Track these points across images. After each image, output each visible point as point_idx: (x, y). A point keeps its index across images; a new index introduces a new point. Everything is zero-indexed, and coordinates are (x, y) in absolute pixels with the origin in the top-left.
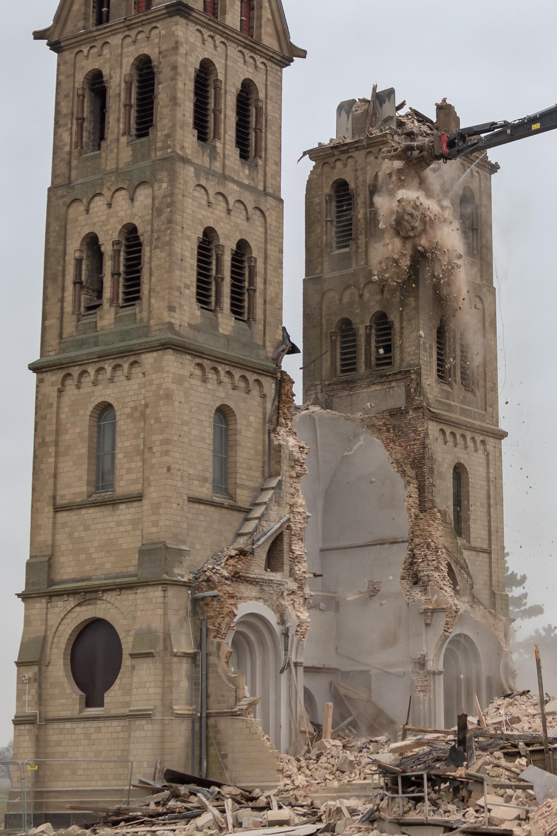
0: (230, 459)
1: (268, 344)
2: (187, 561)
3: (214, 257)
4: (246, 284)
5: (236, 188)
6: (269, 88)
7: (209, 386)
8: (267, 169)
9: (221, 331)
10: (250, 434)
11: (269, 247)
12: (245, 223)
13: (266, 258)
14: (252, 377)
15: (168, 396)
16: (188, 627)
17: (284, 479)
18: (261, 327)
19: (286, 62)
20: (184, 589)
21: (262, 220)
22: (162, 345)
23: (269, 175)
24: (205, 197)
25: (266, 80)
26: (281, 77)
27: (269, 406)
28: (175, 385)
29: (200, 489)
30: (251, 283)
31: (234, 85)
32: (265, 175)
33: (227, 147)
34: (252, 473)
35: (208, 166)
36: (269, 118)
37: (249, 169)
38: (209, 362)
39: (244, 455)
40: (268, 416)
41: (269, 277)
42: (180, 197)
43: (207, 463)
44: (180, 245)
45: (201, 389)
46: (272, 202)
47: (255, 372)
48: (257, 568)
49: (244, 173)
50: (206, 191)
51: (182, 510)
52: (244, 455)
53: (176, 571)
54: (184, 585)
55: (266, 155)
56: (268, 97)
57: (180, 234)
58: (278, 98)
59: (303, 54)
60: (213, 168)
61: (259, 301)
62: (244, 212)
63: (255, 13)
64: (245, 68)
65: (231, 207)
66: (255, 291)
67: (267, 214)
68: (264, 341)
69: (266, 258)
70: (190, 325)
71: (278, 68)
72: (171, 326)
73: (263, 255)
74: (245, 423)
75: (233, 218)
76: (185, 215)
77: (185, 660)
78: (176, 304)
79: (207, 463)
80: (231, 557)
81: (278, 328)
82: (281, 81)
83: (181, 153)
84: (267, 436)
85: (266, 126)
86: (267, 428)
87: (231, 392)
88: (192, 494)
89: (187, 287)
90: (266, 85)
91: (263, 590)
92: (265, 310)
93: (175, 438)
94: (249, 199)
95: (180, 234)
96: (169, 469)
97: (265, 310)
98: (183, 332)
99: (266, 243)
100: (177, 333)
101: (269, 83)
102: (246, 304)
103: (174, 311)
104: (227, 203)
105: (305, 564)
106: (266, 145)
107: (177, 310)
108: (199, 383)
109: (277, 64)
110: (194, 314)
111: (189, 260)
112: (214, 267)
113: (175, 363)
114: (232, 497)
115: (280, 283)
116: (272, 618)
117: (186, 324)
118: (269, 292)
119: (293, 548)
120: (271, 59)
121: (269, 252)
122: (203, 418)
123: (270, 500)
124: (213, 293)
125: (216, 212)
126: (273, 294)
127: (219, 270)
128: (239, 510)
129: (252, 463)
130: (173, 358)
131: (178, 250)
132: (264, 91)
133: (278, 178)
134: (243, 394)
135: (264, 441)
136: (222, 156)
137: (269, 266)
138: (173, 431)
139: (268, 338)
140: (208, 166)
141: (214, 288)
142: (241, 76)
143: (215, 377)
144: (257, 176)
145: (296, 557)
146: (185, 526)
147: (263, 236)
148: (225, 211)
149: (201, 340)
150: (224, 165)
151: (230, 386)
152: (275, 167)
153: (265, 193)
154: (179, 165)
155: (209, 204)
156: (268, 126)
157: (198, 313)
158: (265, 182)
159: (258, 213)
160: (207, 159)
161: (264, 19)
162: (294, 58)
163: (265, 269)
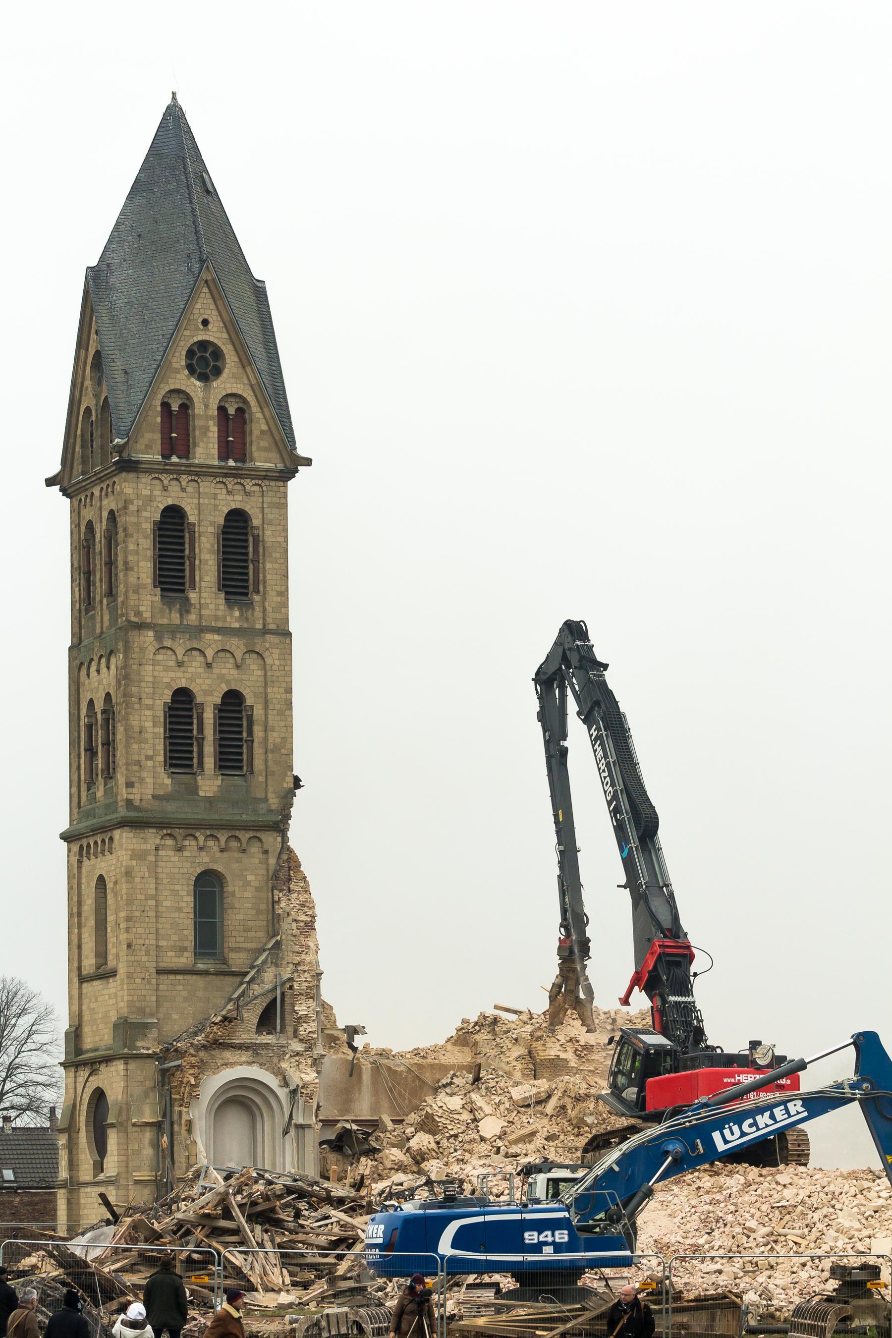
0: (225, 923)
1: (270, 795)
2: (153, 1034)
3: (195, 716)
4: (245, 735)
5: (216, 637)
6: (266, 510)
7: (186, 854)
9: (201, 794)
11: (269, 690)
12: (234, 672)
14: (244, 836)
15: (128, 874)
16: (154, 1097)
17: (284, 937)
18: (261, 779)
19: (289, 473)
20: (149, 1061)
21: (260, 661)
22: (119, 823)
23: (269, 609)
24: (174, 657)
25: (263, 502)
26: (286, 494)
27: (272, 861)
28: (134, 863)
29: (176, 960)
30: (250, 733)
31: (212, 523)
32: (264, 610)
33: (204, 595)
35: (178, 622)
36: (268, 544)
37: (240, 610)
38: (181, 831)
39: (238, 917)
40: (271, 873)
41: (270, 723)
42: (135, 667)
43: (185, 932)
44: (137, 717)
45: (176, 859)
46: (275, 639)
47: (250, 830)
48: (247, 1033)
49: (232, 616)
50: (173, 651)
51: (149, 983)
52: (238, 917)
53: (139, 1044)
54: (149, 1056)
55: (265, 587)
56: (266, 522)
57: (137, 706)
58: (282, 518)
59: (308, 462)
60: (185, 622)
61: (258, 751)
62: (232, 660)
63: (247, 427)
64: (230, 498)
65: (210, 660)
66: (252, 741)
67: (266, 655)
68: (266, 793)
70: (154, 797)
71: (281, 484)
72: (129, 803)
73: (262, 700)
74: (241, 883)
75: (215, 671)
76: (143, 684)
77: (148, 1129)
78: (133, 779)
79: (185, 932)
80: (216, 1024)
81: (286, 776)
82: (286, 497)
83: (136, 620)
84: (270, 894)
85: (264, 556)
86: (270, 885)
87: (218, 854)
88: (163, 965)
89: (149, 758)
90: (263, 508)
91: (257, 1053)
92: (266, 761)
93: (137, 914)
94: (237, 645)
95: (137, 706)
96: (129, 946)
97: (266, 761)
99: (266, 686)
100: (138, 809)
101: (265, 506)
102: (245, 757)
103: (133, 787)
104: (205, 656)
105: (312, 1024)
106: (264, 577)
107: (136, 785)
108: (171, 853)
109: (276, 480)
110: (163, 784)
111: (150, 730)
112: (195, 727)
113: (134, 840)
114: (225, 962)
115: (289, 727)
116: (272, 1081)
117: (150, 797)
118: (270, 740)
119: (296, 1008)
120: (265, 478)
121: (269, 696)
122: (178, 887)
123: (264, 962)
124: (195, 755)
125: (190, 670)
126: (278, 740)
127: (201, 730)
128: (234, 974)
129: (251, 923)
130: (131, 835)
131: (135, 723)
132: (260, 516)
133: (283, 610)
134: (236, 855)
135: (268, 898)
136: (198, 606)
137: (270, 712)
138: (134, 907)
139: (270, 789)
140: (178, 622)
141: (195, 749)
142: (224, 508)
143: (194, 843)
144: (253, 615)
145: (300, 1018)
146: (154, 998)
147: (262, 679)
148: (204, 665)
149: (171, 809)
150: (200, 616)
151: (216, 849)
152: (279, 599)
153: (265, 631)
154: (133, 635)
155: (180, 664)
156: (267, 555)
157: (168, 781)
158: (264, 619)
159: (254, 656)
161: (256, 433)
162: (299, 468)
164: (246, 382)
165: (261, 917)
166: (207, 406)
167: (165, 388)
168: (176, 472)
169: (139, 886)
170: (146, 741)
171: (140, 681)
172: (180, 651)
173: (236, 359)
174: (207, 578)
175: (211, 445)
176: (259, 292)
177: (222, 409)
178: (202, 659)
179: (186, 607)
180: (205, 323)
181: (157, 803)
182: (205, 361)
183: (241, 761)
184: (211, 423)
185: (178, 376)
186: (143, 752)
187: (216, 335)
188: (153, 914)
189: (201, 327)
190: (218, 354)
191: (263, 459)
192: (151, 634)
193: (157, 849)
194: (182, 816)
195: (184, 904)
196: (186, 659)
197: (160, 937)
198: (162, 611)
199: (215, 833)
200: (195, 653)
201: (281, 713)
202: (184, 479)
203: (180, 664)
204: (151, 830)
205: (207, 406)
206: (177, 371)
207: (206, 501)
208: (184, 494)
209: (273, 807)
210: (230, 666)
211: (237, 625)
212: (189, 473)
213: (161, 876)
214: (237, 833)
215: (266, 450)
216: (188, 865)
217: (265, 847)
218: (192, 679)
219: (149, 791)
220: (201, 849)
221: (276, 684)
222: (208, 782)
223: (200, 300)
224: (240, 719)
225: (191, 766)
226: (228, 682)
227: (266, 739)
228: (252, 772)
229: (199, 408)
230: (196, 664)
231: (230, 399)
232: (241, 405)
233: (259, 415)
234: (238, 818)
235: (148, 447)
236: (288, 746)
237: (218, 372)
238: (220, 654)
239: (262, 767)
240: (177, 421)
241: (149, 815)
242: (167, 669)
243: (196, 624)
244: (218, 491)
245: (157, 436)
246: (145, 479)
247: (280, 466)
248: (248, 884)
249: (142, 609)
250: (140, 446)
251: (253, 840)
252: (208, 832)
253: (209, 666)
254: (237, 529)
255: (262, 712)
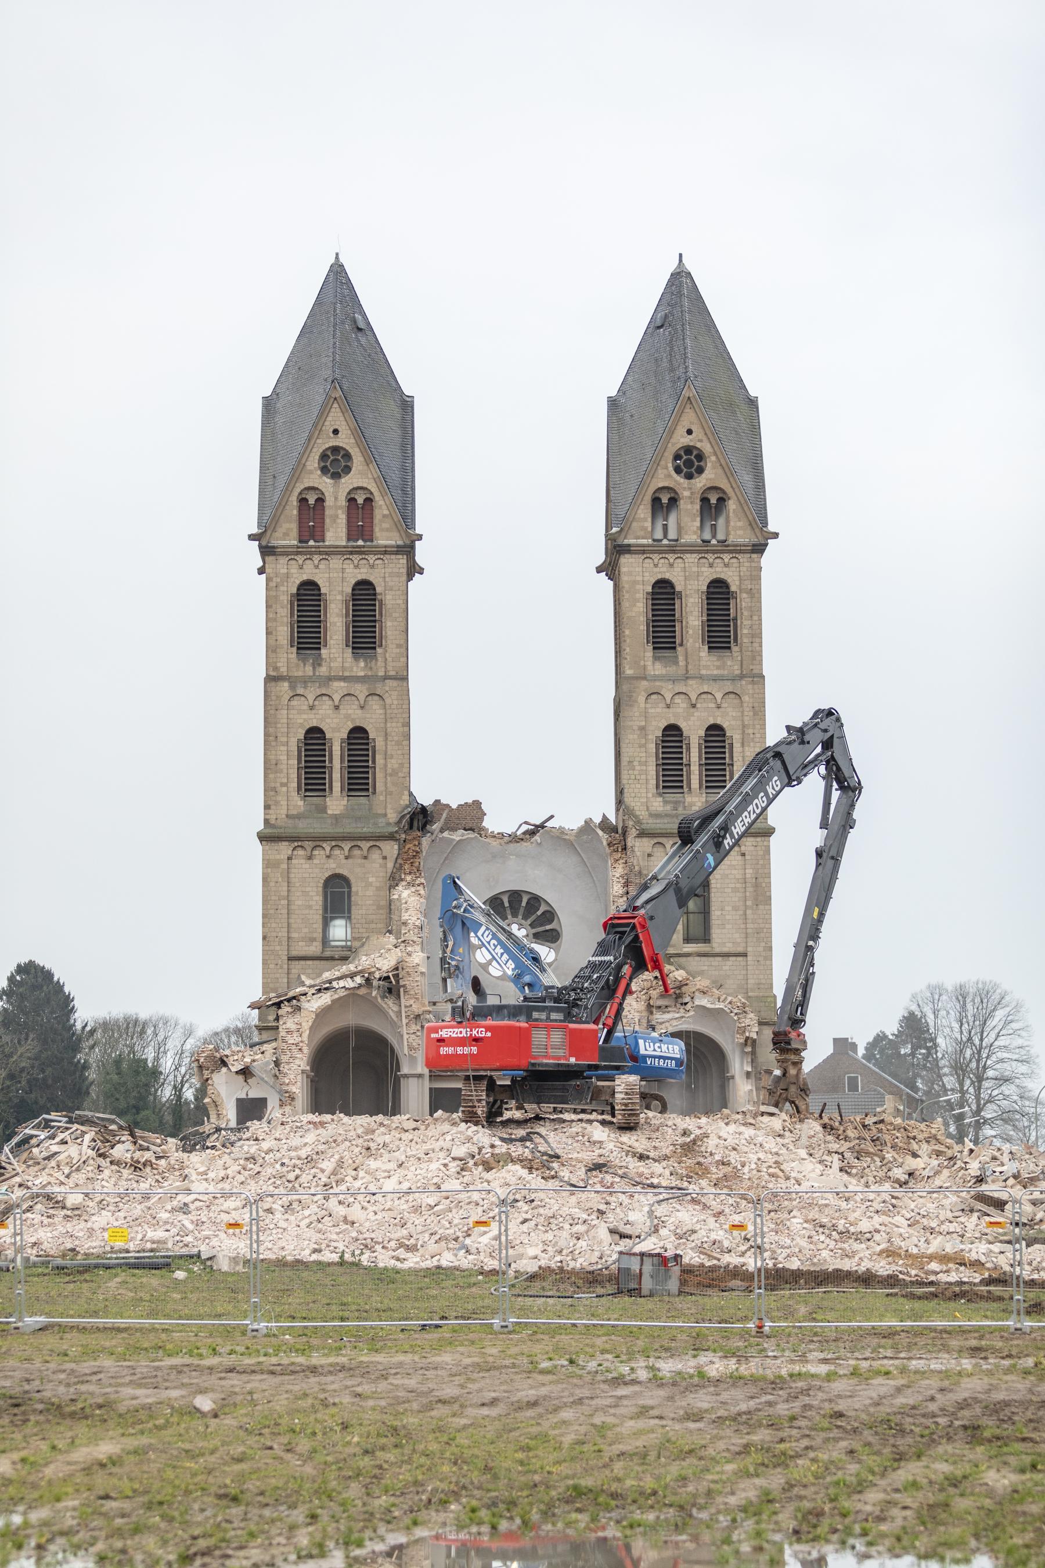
1: (389, 811)
5: (342, 684)
7: (315, 861)
8: (387, 655)
9: (329, 812)
10: (368, 893)
11: (389, 725)
12: (359, 712)
13: (386, 734)
14: (365, 845)
18: (382, 798)
21: (381, 702)
23: (389, 659)
27: (390, 865)
28: (269, 870)
29: (307, 948)
30: (374, 762)
34: (373, 926)
35: (311, 674)
37: (365, 661)
39: (360, 912)
40: (389, 875)
43: (315, 926)
45: (307, 866)
46: (394, 683)
51: (281, 968)
52: (360, 912)
57: (273, 744)
61: (379, 775)
62: (356, 702)
64: (358, 571)
69: (386, 734)
70: (287, 816)
74: (363, 884)
75: (342, 711)
76: (279, 725)
79: (315, 926)
83: (274, 674)
88: (294, 953)
89: (282, 785)
92: (386, 784)
93: (272, 912)
94: (361, 690)
95: (273, 744)
98: (279, 823)
100: (273, 826)
108: (303, 861)
118: (389, 766)
120: (385, 553)
121: (389, 730)
122: (308, 889)
125: (320, 712)
127: (331, 761)
131: (273, 757)
134: (360, 861)
139: (389, 806)
140: (311, 674)
143: (322, 852)
147: (383, 716)
148: (332, 707)
149: (303, 827)
151: (342, 857)
153: (386, 678)
157: (301, 803)
159: (377, 698)
160: (309, 670)
163: (386, 745)
164: (370, 476)
165: (381, 912)
166: (336, 498)
167: (300, 487)
168: (310, 554)
169: (273, 889)
170: (281, 771)
171: (276, 723)
172: (311, 697)
173: (362, 459)
174: (335, 637)
175: (339, 530)
176: (407, 405)
177: (351, 501)
178: (331, 703)
179: (318, 662)
180: (336, 432)
181: (290, 821)
182: (336, 463)
183: (368, 784)
184: (340, 512)
185: (312, 476)
186: (279, 780)
187: (346, 441)
188: (285, 911)
189: (332, 435)
190: (348, 456)
191: (385, 536)
192: (286, 684)
193: (289, 858)
194: (312, 831)
195: (314, 903)
196: (316, 703)
197: (292, 930)
198: (297, 665)
199: (340, 843)
200: (324, 698)
201: (398, 743)
202: (316, 558)
203: (312, 708)
204: (284, 843)
205: (336, 498)
206: (311, 472)
207: (335, 575)
208: (317, 571)
209: (391, 821)
210: (355, 707)
211: (362, 674)
212: (320, 553)
213: (293, 880)
214: (359, 843)
215: (387, 530)
216: (317, 871)
217: (384, 854)
218: (322, 720)
219: (284, 812)
220: (328, 857)
221: (395, 720)
222: (335, 803)
223: (331, 414)
224: (368, 750)
225: (325, 790)
226: (353, 720)
227: (386, 765)
228: (374, 793)
229: (329, 502)
230: (325, 707)
231: (359, 491)
232: (368, 496)
233: (381, 503)
234: (359, 830)
235: (286, 535)
236: (406, 770)
237: (348, 469)
238: (347, 698)
239: (383, 788)
240: (311, 512)
241: (282, 830)
242: (300, 712)
243: (327, 674)
244: (345, 566)
245: (294, 527)
246: (283, 560)
247: (400, 543)
248: (371, 884)
249: (279, 665)
250: (279, 533)
251: (374, 849)
252: (334, 843)
253: (337, 708)
254: (364, 595)
255: (383, 743)
